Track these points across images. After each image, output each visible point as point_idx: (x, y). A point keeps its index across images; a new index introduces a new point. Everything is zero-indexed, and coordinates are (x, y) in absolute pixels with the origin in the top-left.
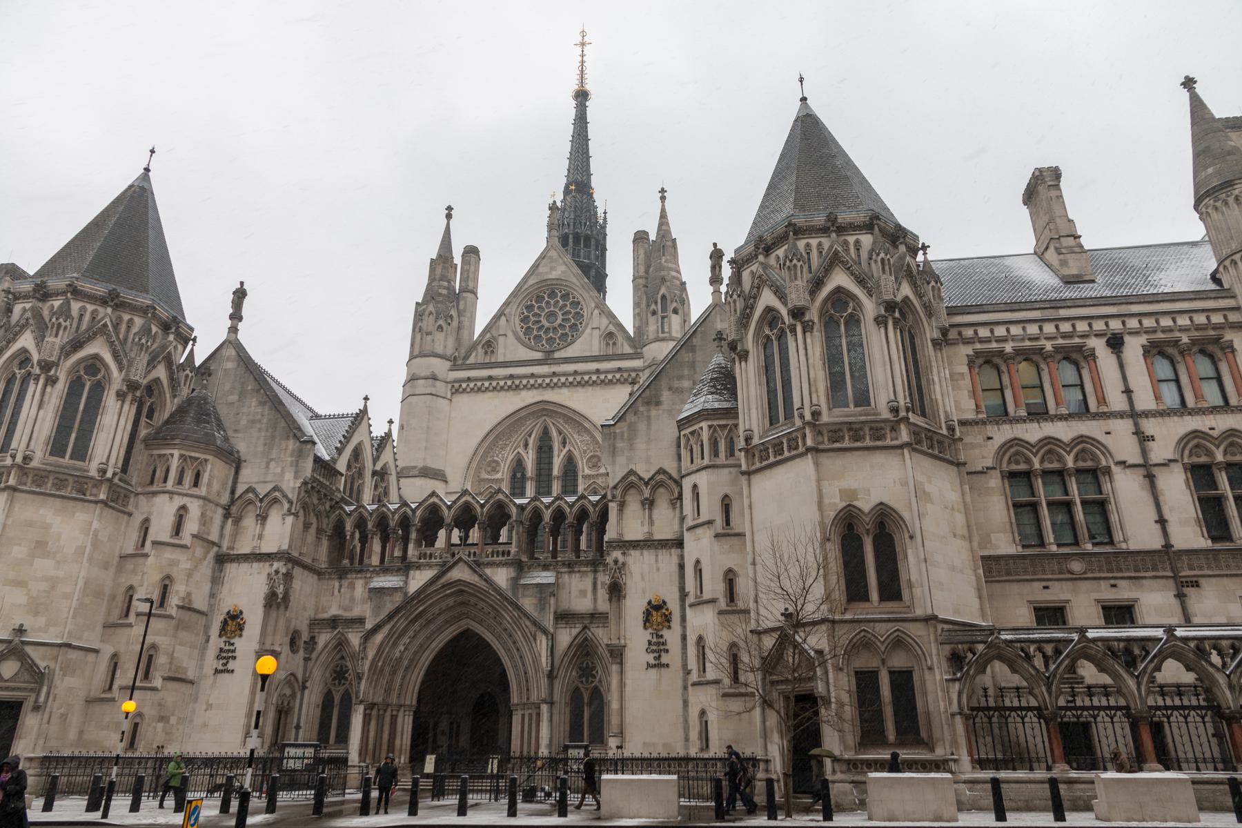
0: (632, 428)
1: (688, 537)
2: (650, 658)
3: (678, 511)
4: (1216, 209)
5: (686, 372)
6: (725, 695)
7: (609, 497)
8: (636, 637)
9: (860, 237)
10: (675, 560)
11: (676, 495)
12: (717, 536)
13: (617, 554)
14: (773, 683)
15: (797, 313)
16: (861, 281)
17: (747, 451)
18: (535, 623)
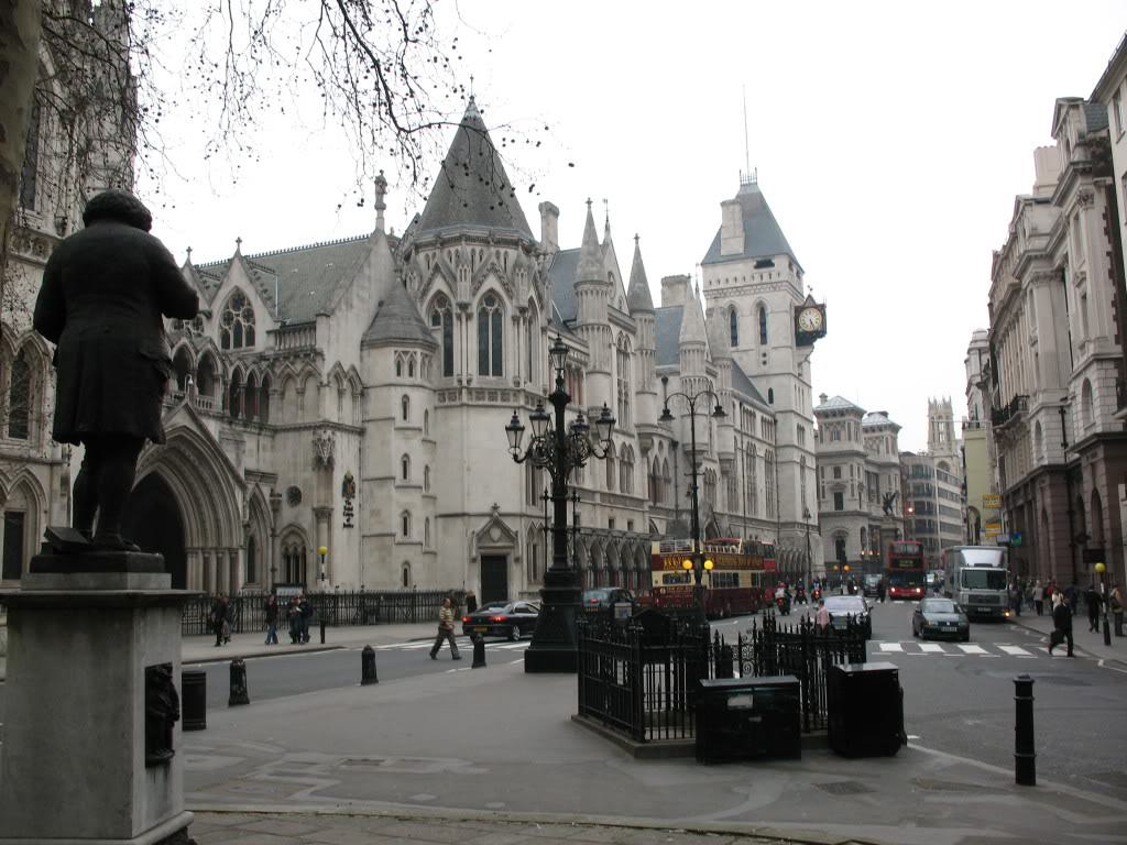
0: (338, 325)
1: (370, 427)
2: (344, 519)
3: (358, 403)
4: (592, 292)
5: (366, 284)
6: (426, 553)
7: (325, 382)
8: (339, 503)
9: (509, 250)
10: (357, 443)
11: (359, 392)
12: (424, 441)
13: (329, 432)
14: (480, 548)
15: (523, 310)
16: (540, 298)
17: (468, 388)
18: (237, 477)
